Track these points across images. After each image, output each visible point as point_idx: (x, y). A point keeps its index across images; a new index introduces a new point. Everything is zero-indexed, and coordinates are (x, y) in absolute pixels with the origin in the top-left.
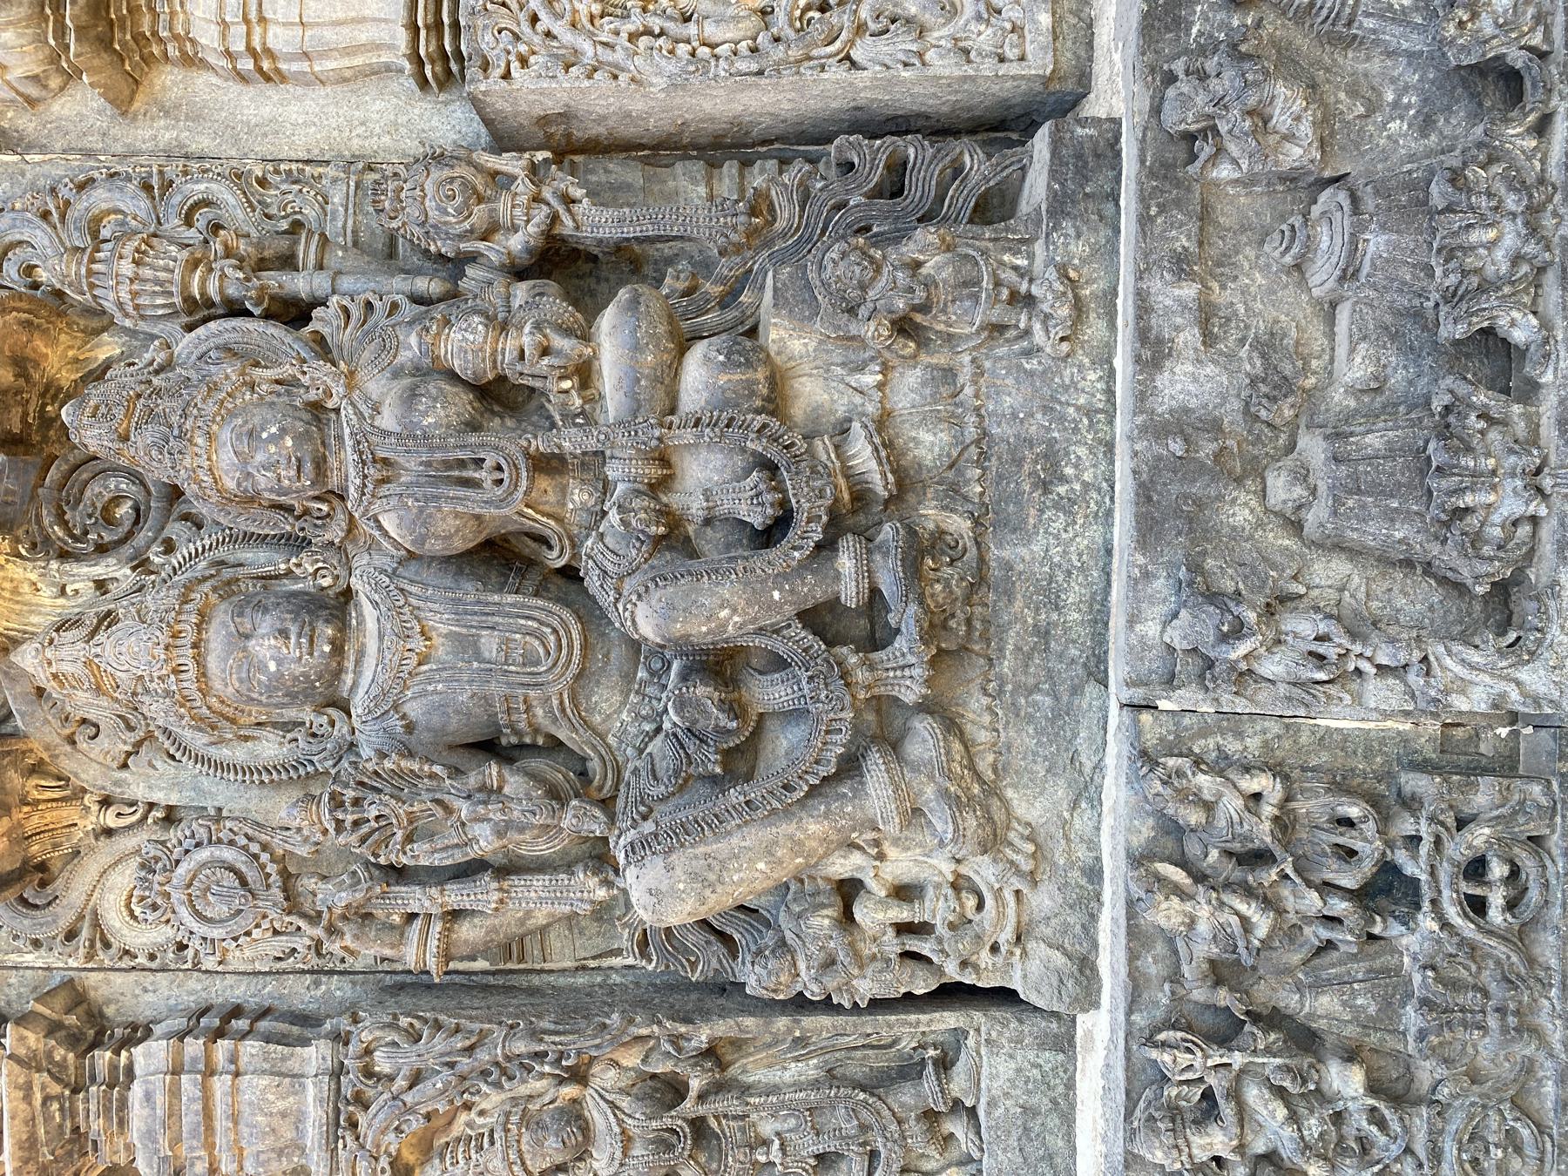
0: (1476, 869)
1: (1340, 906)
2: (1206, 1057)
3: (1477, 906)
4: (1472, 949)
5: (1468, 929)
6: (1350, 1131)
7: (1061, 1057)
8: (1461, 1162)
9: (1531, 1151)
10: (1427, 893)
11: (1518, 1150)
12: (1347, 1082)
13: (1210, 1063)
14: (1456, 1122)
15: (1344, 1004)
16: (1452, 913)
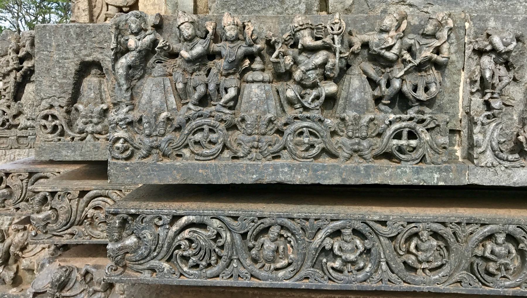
0: (412, 135)
1: (397, 84)
2: (338, 35)
3: (398, 136)
4: (379, 135)
5: (389, 132)
6: (308, 91)
7: (303, 12)
8: (302, 127)
9: (306, 154)
10: (404, 116)
11: (307, 150)
12: (330, 88)
13: (335, 36)
14: (316, 126)
15: (356, 89)
16: (397, 125)
